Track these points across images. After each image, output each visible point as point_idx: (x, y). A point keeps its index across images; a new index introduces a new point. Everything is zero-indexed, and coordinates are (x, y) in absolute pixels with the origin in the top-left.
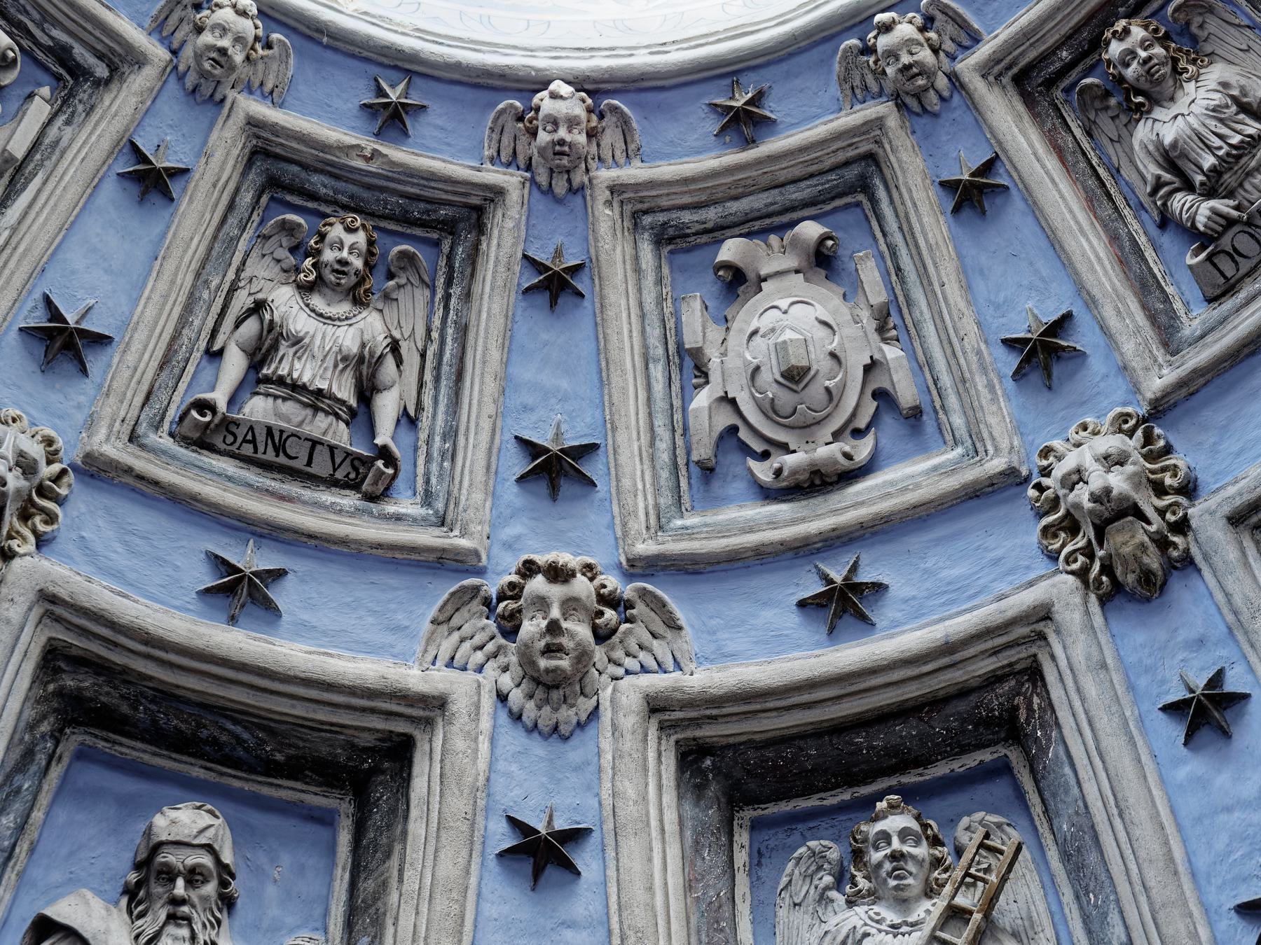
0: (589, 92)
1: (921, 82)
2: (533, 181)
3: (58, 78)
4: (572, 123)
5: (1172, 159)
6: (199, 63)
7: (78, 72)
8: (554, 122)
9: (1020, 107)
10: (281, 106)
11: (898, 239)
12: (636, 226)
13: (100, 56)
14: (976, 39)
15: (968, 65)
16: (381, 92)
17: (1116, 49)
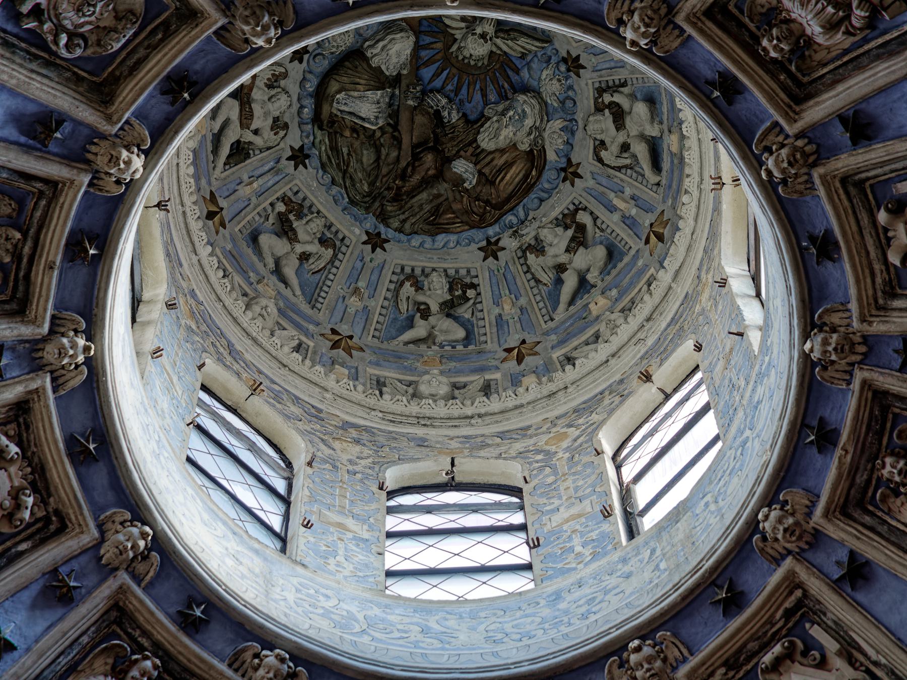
0: (812, 330)
1: (798, 156)
2: (859, 363)
3: (803, 615)
4: (825, 342)
5: (831, 27)
6: (792, 542)
7: (799, 604)
8: (825, 352)
9: (811, 103)
10: (818, 497)
11: (887, 168)
12: (884, 308)
13: (791, 593)
14: (776, 124)
15: (791, 129)
16: (812, 442)
17: (773, 54)
